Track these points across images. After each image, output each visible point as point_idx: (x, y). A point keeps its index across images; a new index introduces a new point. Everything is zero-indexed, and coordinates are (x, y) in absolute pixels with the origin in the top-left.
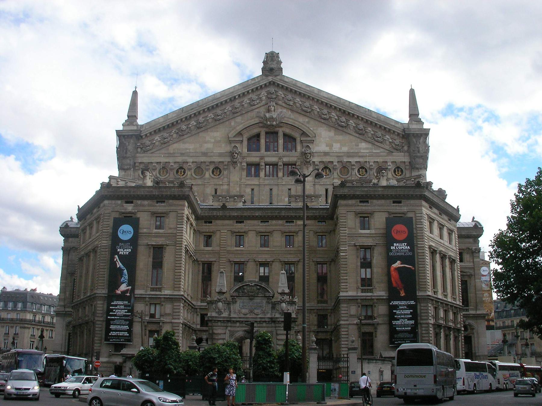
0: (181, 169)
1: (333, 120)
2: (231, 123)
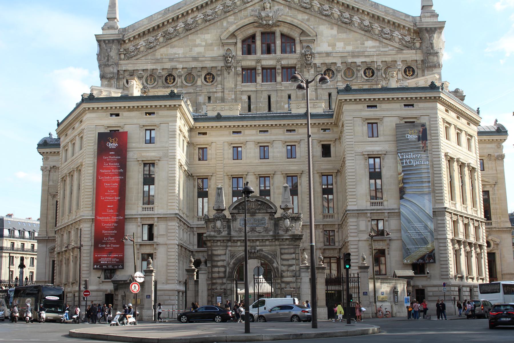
0: (170, 77)
1: (336, 16)
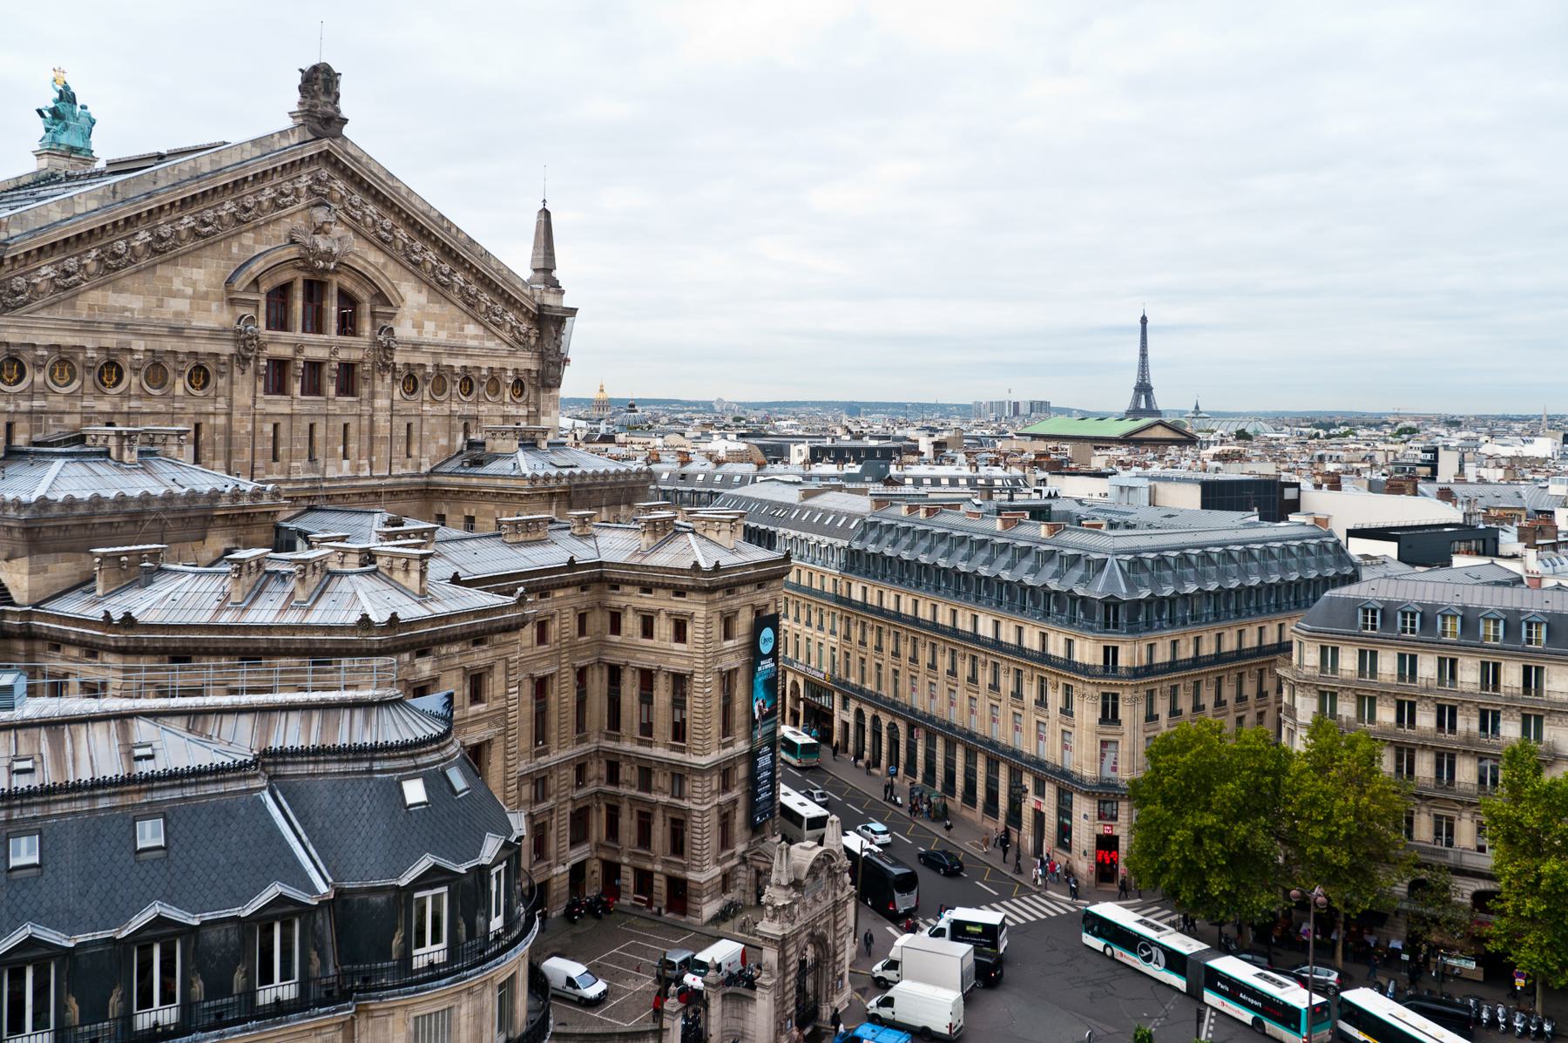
1: (429, 266)
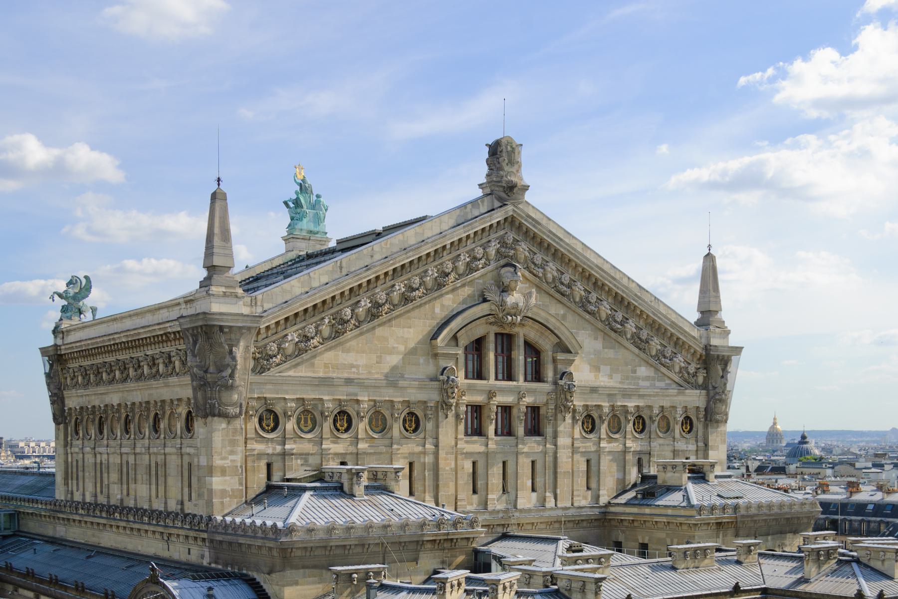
0: (344, 420)
1: (604, 316)
2: (434, 308)
